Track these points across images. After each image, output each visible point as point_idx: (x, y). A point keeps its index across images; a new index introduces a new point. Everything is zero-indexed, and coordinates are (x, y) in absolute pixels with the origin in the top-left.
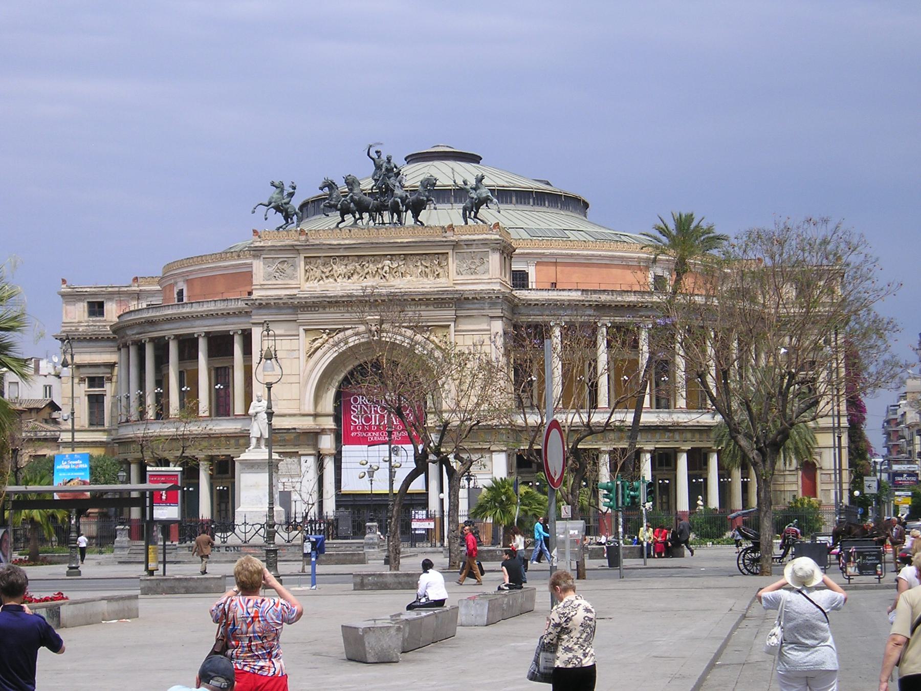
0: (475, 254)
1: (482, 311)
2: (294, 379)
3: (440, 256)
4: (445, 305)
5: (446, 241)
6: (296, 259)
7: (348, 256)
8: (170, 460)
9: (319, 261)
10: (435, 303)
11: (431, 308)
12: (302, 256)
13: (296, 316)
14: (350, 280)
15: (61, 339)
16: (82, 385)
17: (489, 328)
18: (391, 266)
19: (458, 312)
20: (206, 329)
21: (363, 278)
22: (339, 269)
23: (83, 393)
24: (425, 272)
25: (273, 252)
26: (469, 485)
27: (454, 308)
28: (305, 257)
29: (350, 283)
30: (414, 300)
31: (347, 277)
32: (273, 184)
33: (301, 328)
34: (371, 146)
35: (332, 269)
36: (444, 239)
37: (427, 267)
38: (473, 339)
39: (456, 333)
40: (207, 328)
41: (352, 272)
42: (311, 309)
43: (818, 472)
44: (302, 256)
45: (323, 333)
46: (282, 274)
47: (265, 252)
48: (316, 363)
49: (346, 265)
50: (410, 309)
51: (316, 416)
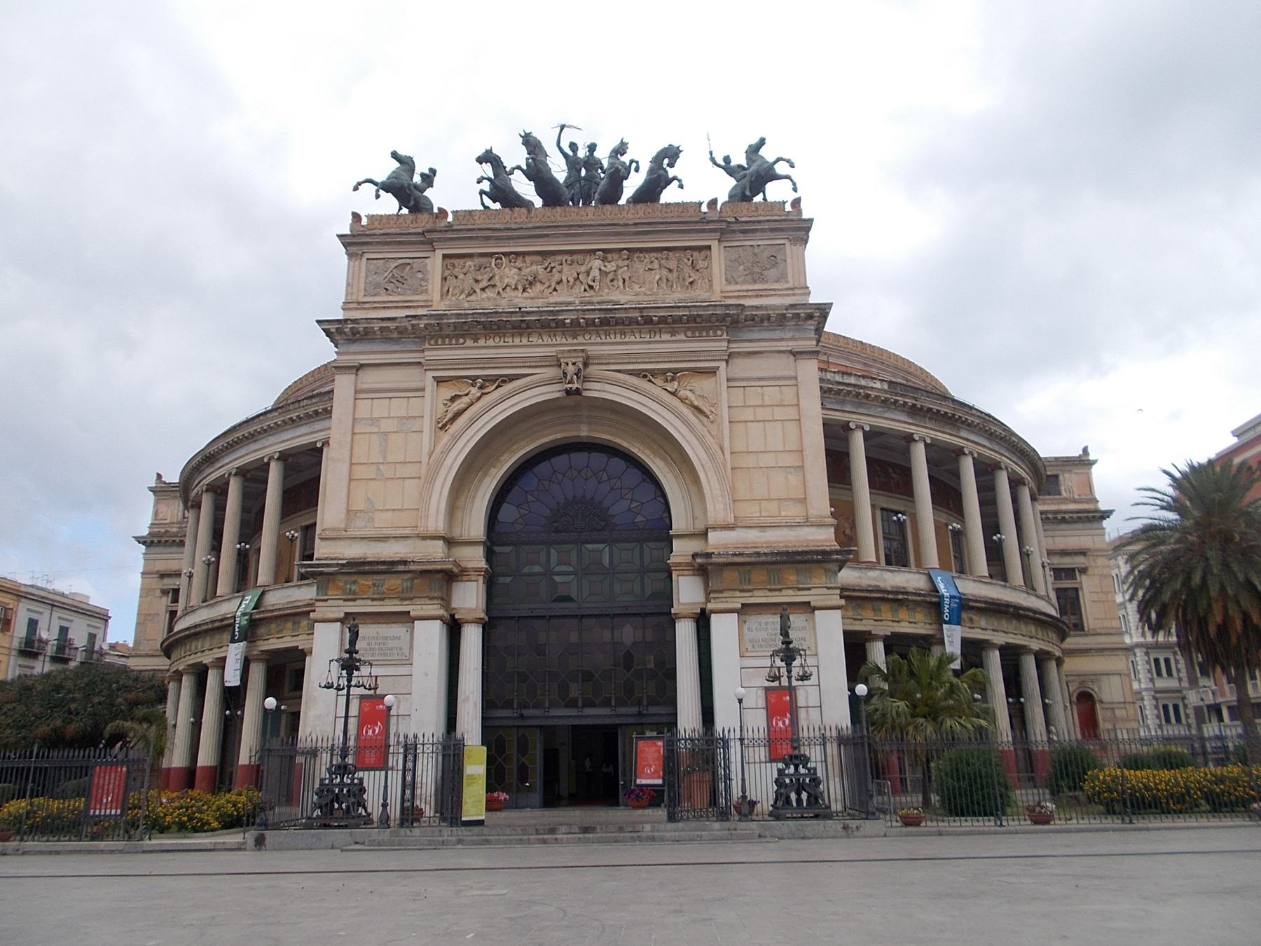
0: (762, 248)
1: (778, 344)
2: (410, 470)
3: (695, 254)
4: (707, 333)
6: (427, 261)
7: (524, 254)
8: (209, 665)
9: (469, 263)
11: (682, 337)
12: (439, 254)
13: (421, 355)
14: (525, 294)
15: (144, 543)
16: (164, 599)
17: (793, 374)
18: (603, 268)
19: (732, 345)
20: (283, 447)
21: (550, 290)
22: (509, 273)
23: (164, 607)
24: (667, 280)
25: (386, 247)
26: (789, 671)
27: (725, 336)
28: (445, 256)
29: (526, 298)
30: (648, 321)
31: (520, 287)
32: (395, 155)
33: (431, 374)
34: (562, 127)
37: (670, 271)
38: (763, 395)
39: (731, 384)
40: (282, 445)
41: (530, 279)
42: (451, 340)
43: (1098, 706)
44: (439, 254)
45: (472, 385)
47: (371, 247)
48: (456, 439)
49: (520, 269)
50: (641, 340)
51: (450, 542)
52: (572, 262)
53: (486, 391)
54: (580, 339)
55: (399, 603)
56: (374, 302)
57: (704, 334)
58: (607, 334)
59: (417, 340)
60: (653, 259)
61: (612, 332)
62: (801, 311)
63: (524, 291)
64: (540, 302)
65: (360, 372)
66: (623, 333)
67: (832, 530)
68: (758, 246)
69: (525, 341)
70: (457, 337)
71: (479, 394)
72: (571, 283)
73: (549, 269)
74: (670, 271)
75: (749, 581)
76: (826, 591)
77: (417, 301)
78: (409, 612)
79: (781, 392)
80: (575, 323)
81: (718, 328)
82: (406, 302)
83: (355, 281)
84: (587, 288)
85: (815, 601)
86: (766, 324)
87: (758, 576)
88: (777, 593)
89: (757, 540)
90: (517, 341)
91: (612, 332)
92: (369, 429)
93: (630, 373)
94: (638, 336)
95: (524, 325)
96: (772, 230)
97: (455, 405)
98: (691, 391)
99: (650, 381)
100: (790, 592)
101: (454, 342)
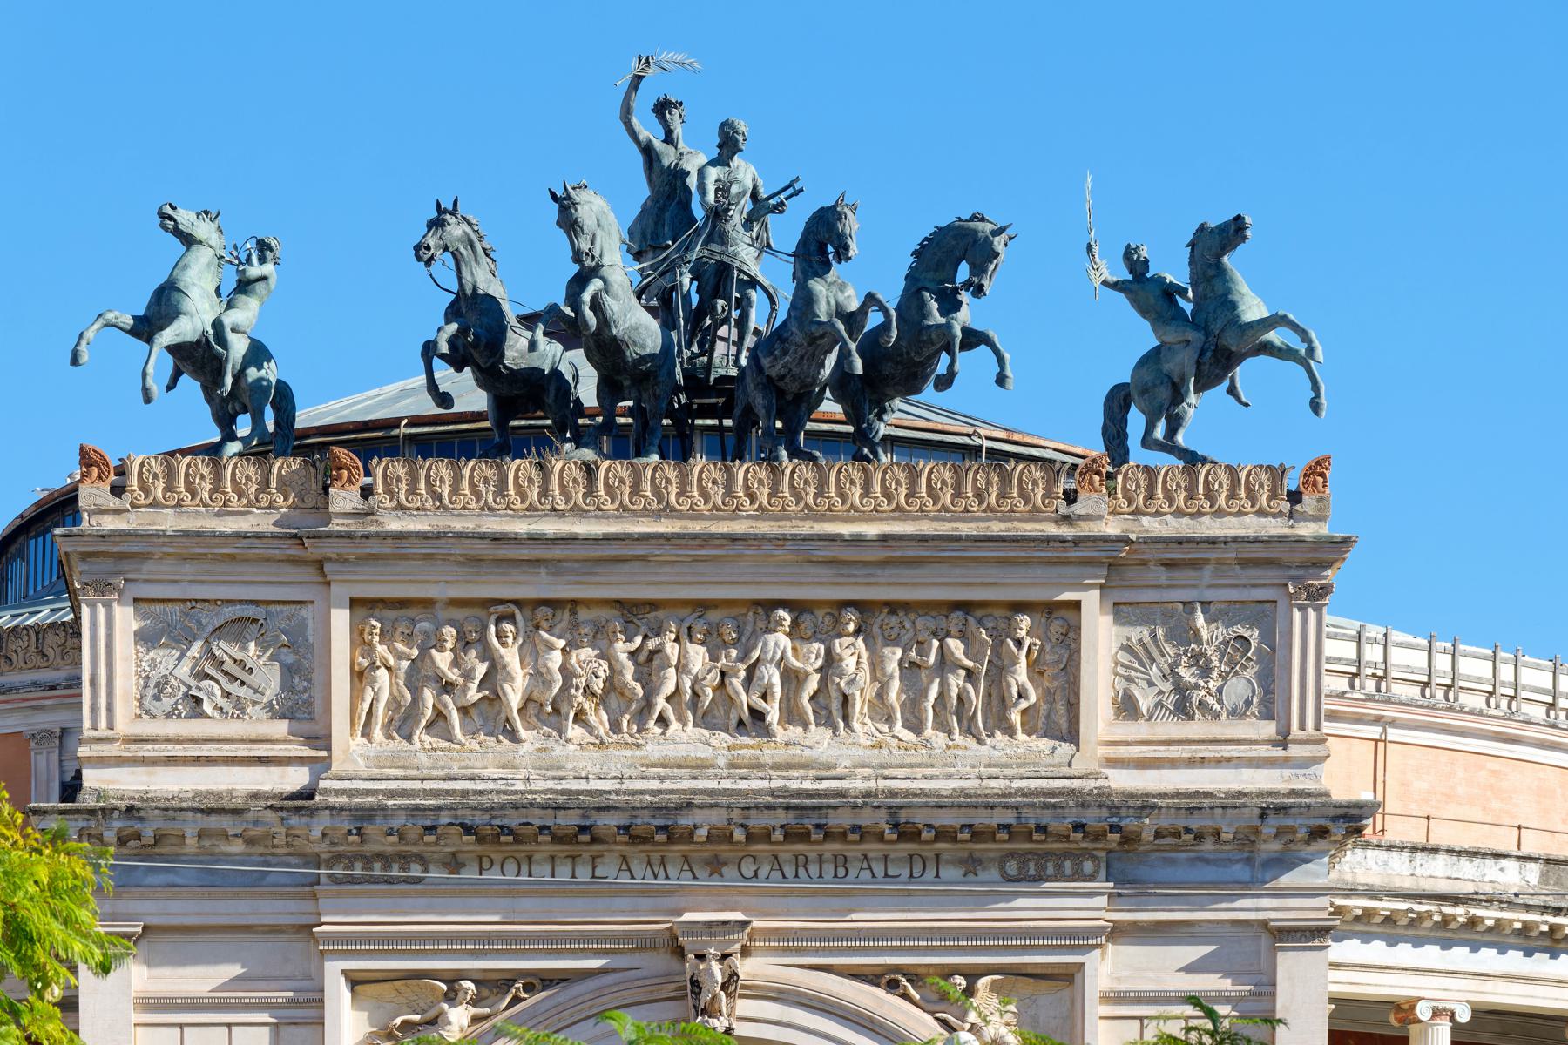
4: (1059, 867)
5: (1077, 542)
6: (306, 612)
7: (575, 603)
10: (1012, 854)
25: (188, 568)
36: (1065, 531)
46: (234, 688)
47: (148, 567)
54: (731, 872)
56: (168, 741)
57: (1050, 870)
58: (801, 862)
61: (812, 856)
62: (1300, 821)
64: (619, 760)
66: (841, 862)
68: (1202, 603)
70: (404, 859)
80: (720, 836)
81: (1088, 854)
86: (1208, 846)
94: (879, 869)
95: (585, 838)
96: (1245, 563)
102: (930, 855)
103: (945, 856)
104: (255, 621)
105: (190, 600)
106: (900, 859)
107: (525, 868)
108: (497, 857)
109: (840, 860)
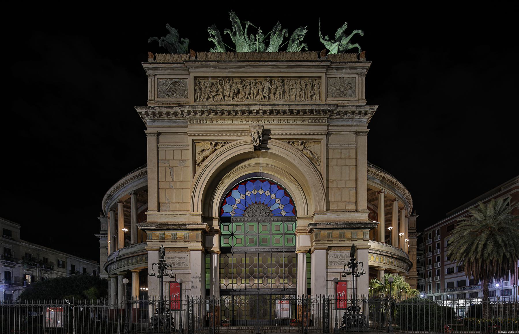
4: (319, 121)
6: (187, 80)
9: (208, 82)
11: (307, 122)
12: (192, 75)
13: (186, 129)
14: (234, 100)
18: (270, 87)
21: (246, 97)
24: (300, 95)
28: (195, 78)
31: (231, 96)
35: (219, 89)
38: (341, 153)
44: (192, 75)
48: (204, 169)
49: (231, 86)
52: (256, 83)
53: (216, 148)
55: (184, 243)
56: (163, 101)
59: (184, 121)
60: (294, 83)
63: (233, 98)
65: (159, 137)
67: (368, 215)
68: (343, 78)
69: (234, 122)
71: (213, 149)
72: (255, 95)
73: (244, 88)
74: (301, 90)
75: (332, 236)
76: (363, 241)
77: (183, 101)
78: (188, 247)
79: (349, 152)
82: (177, 101)
83: (153, 90)
84: (263, 97)
85: (358, 245)
87: (336, 233)
88: (342, 242)
89: (336, 219)
90: (231, 122)
91: (275, 119)
92: (165, 165)
93: (283, 140)
94: (286, 122)
97: (204, 153)
98: (309, 150)
99: (291, 145)
100: (348, 242)
101: (201, 122)
102: (296, 119)
103: (298, 119)
104: (178, 82)
105: (167, 78)
106: (290, 120)
107: (224, 121)
108: (219, 119)
109: (280, 120)
